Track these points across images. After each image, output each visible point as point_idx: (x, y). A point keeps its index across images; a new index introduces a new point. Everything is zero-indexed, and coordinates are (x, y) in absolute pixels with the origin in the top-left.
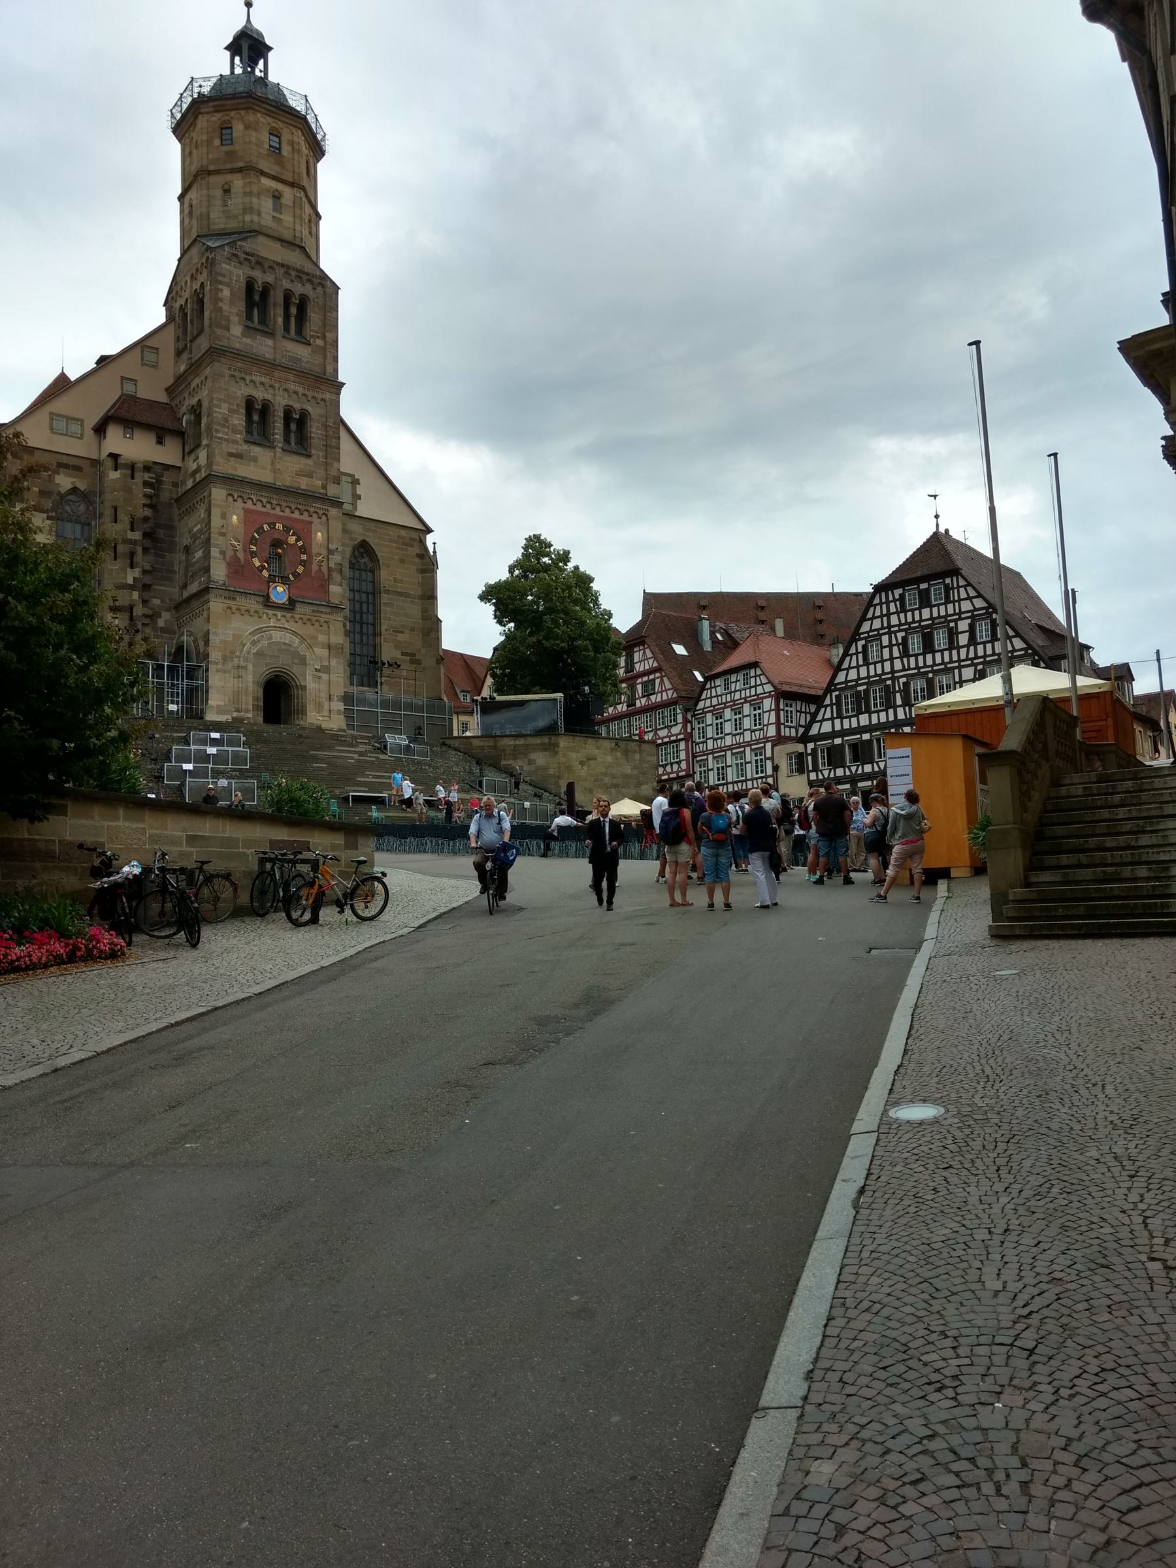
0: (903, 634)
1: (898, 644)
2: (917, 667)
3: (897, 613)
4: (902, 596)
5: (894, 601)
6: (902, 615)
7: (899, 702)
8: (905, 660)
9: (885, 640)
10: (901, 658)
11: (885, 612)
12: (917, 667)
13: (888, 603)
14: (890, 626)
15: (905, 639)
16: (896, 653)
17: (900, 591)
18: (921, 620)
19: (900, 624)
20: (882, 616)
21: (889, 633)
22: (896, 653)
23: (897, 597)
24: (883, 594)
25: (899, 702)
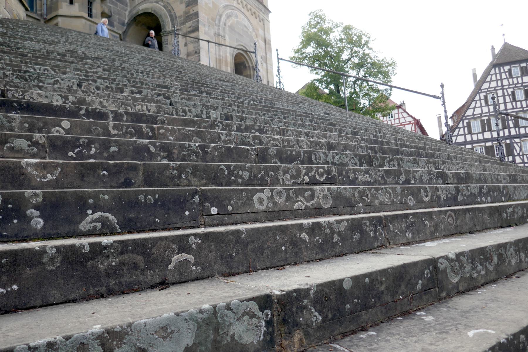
0: (512, 90)
1: (509, 95)
2: (522, 107)
3: (507, 78)
4: (510, 71)
5: (505, 72)
6: (510, 80)
7: (511, 125)
8: (514, 103)
9: (500, 93)
10: (511, 102)
11: (499, 78)
12: (522, 107)
13: (500, 73)
14: (502, 85)
15: (513, 93)
16: (508, 99)
17: (508, 67)
18: (523, 83)
19: (509, 85)
20: (497, 80)
21: (503, 89)
22: (508, 99)
23: (506, 70)
24: (497, 69)
25: (511, 125)
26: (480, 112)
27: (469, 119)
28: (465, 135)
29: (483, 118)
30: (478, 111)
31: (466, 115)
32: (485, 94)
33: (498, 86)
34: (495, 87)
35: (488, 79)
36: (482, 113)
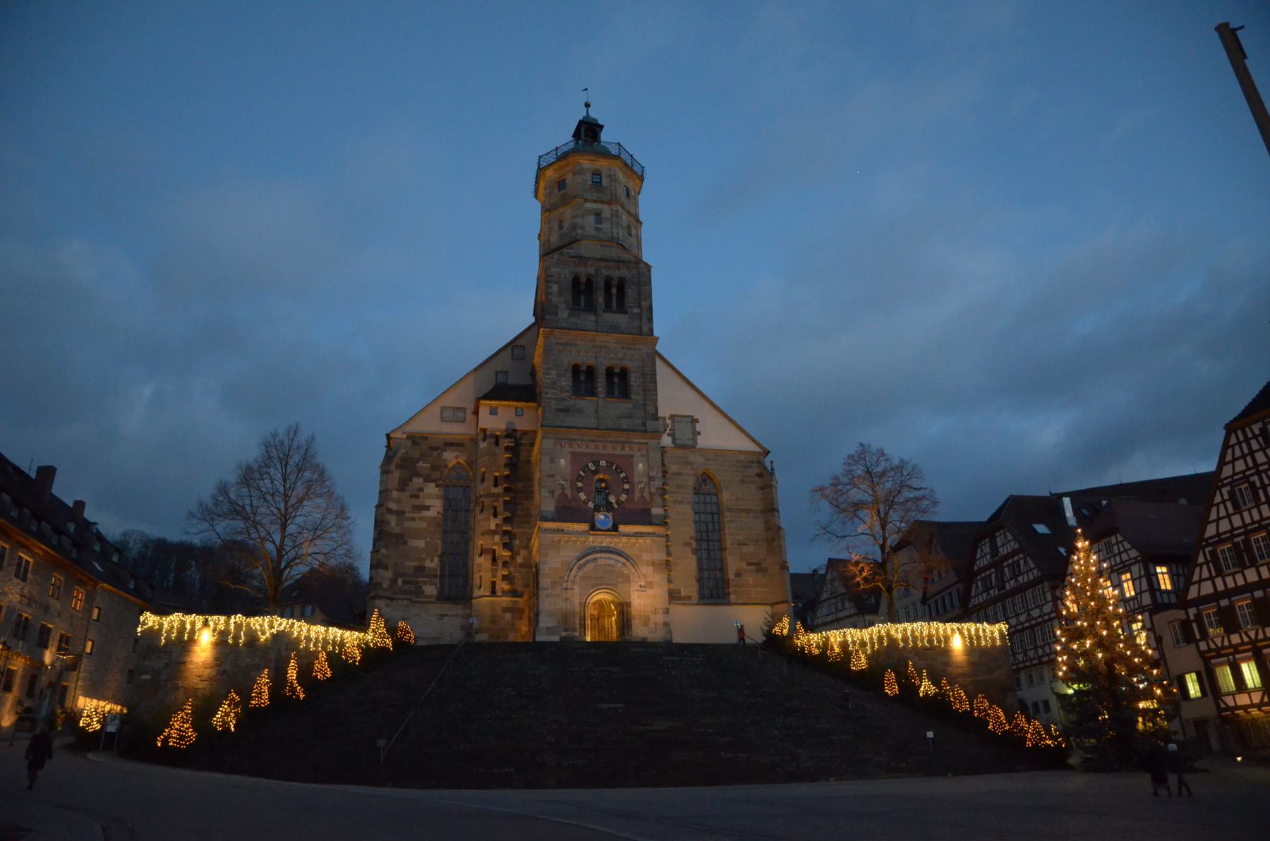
5: (1255, 437)
11: (1246, 451)
13: (1247, 440)
14: (1256, 465)
20: (1243, 457)
23: (1257, 432)
24: (1240, 433)
26: (1229, 528)
27: (1213, 544)
28: (1211, 578)
29: (1236, 540)
30: (1224, 526)
31: (1206, 536)
32: (1228, 488)
33: (1248, 468)
34: (1243, 472)
35: (1229, 458)
36: (1233, 529)
